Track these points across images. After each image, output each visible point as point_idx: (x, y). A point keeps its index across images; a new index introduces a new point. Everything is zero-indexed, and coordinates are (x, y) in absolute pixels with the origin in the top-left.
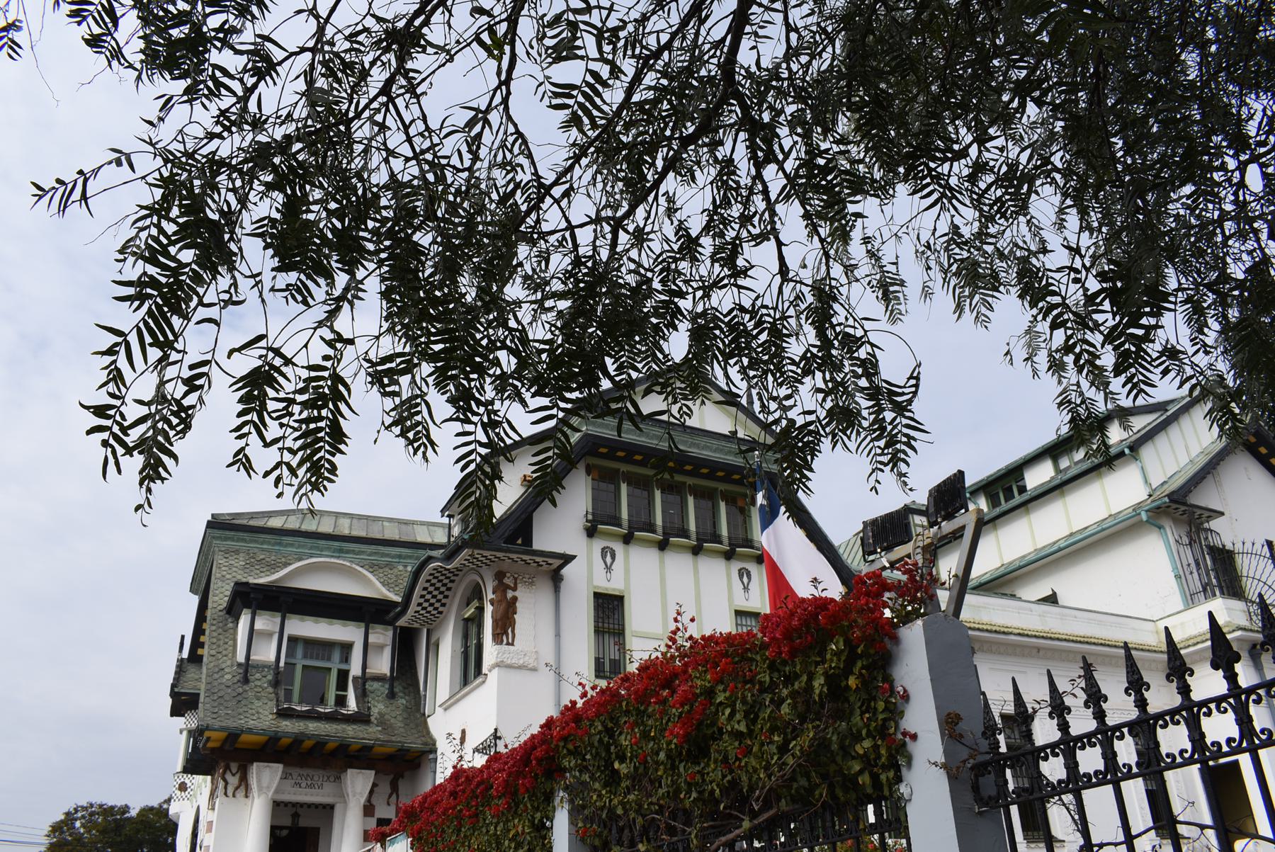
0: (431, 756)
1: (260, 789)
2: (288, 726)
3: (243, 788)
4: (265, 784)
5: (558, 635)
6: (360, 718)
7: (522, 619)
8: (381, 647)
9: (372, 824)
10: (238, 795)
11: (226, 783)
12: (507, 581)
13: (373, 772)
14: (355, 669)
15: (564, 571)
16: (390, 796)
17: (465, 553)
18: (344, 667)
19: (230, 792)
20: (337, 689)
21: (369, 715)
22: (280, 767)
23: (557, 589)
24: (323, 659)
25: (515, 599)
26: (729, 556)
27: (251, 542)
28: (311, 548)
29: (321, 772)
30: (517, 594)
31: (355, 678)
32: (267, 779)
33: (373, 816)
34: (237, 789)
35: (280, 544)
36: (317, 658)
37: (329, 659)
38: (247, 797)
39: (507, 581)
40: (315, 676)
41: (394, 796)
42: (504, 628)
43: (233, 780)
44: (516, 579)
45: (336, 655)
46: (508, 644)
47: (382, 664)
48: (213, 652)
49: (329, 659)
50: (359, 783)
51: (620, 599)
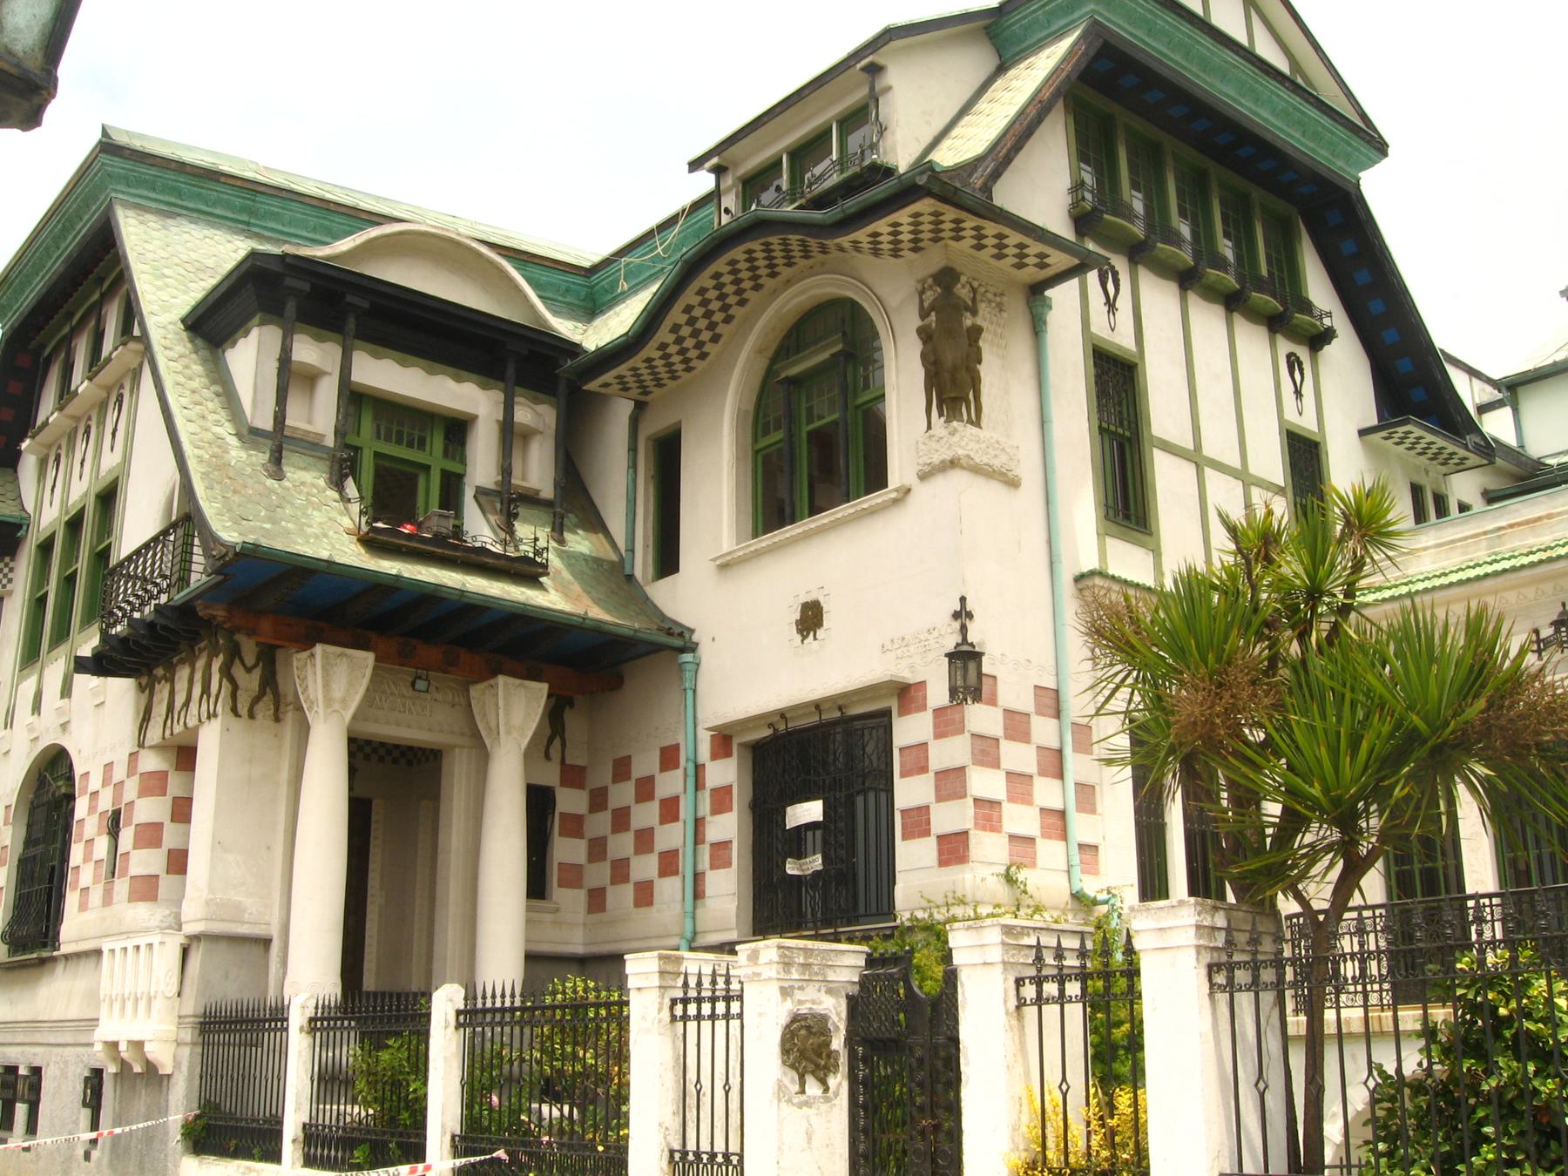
0: (687, 657)
1: (329, 701)
3: (268, 698)
4: (338, 691)
5: (1043, 422)
6: (528, 571)
7: (990, 373)
8: (527, 435)
10: (259, 716)
11: (235, 688)
12: (963, 292)
13: (544, 687)
14: (482, 466)
15: (1048, 293)
16: (550, 741)
17: (925, 206)
18: (453, 467)
19: (243, 708)
21: (545, 566)
22: (368, 658)
23: (1037, 327)
24: (410, 445)
25: (976, 332)
27: (192, 197)
28: (314, 230)
31: (481, 493)
32: (335, 688)
34: (257, 700)
35: (252, 213)
36: (399, 442)
37: (422, 445)
38: (277, 719)
39: (963, 292)
41: (557, 741)
42: (953, 388)
43: (249, 682)
46: (970, 422)
47: (537, 470)
48: (184, 401)
49: (422, 445)
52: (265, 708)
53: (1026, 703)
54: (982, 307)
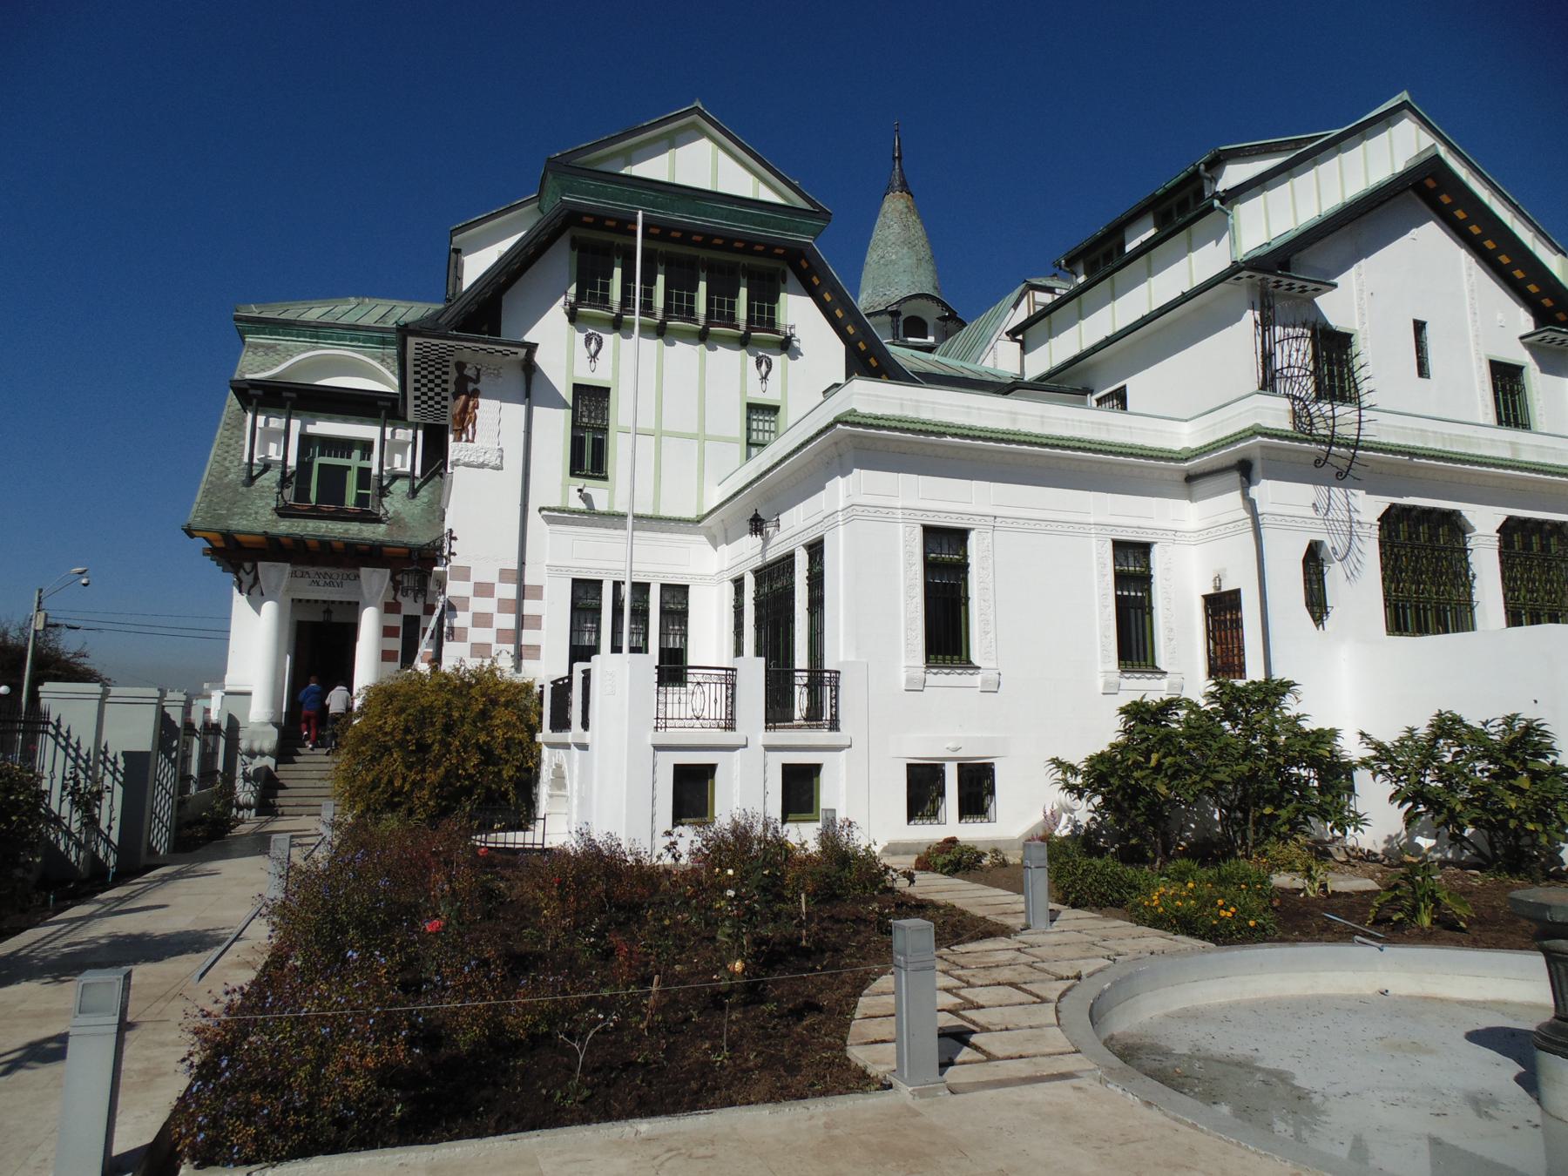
2: (284, 527)
9: (396, 621)
12: (470, 372)
18: (365, 464)
20: (359, 487)
22: (287, 567)
26: (744, 342)
29: (340, 571)
30: (478, 386)
33: (399, 612)
37: (349, 457)
39: (470, 372)
40: (333, 477)
44: (478, 370)
45: (356, 454)
49: (349, 457)
50: (375, 580)
51: (607, 390)
52: (255, 591)
53: (493, 577)
54: (483, 378)
